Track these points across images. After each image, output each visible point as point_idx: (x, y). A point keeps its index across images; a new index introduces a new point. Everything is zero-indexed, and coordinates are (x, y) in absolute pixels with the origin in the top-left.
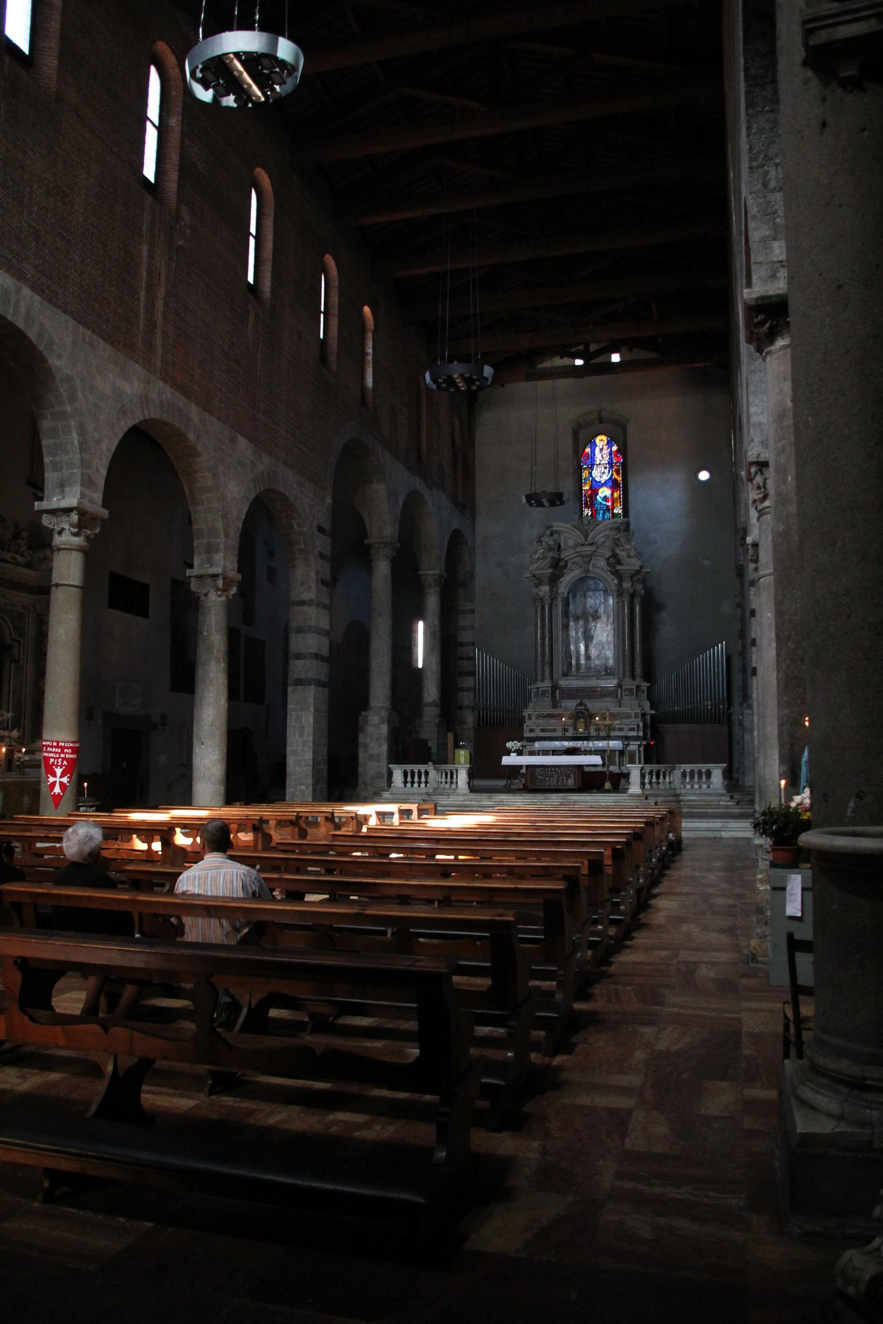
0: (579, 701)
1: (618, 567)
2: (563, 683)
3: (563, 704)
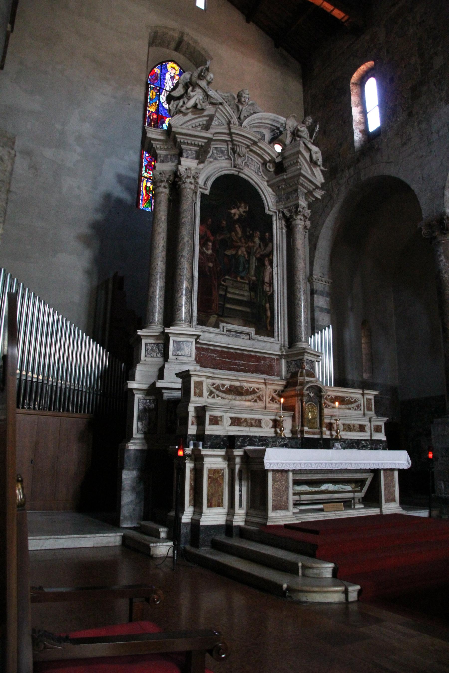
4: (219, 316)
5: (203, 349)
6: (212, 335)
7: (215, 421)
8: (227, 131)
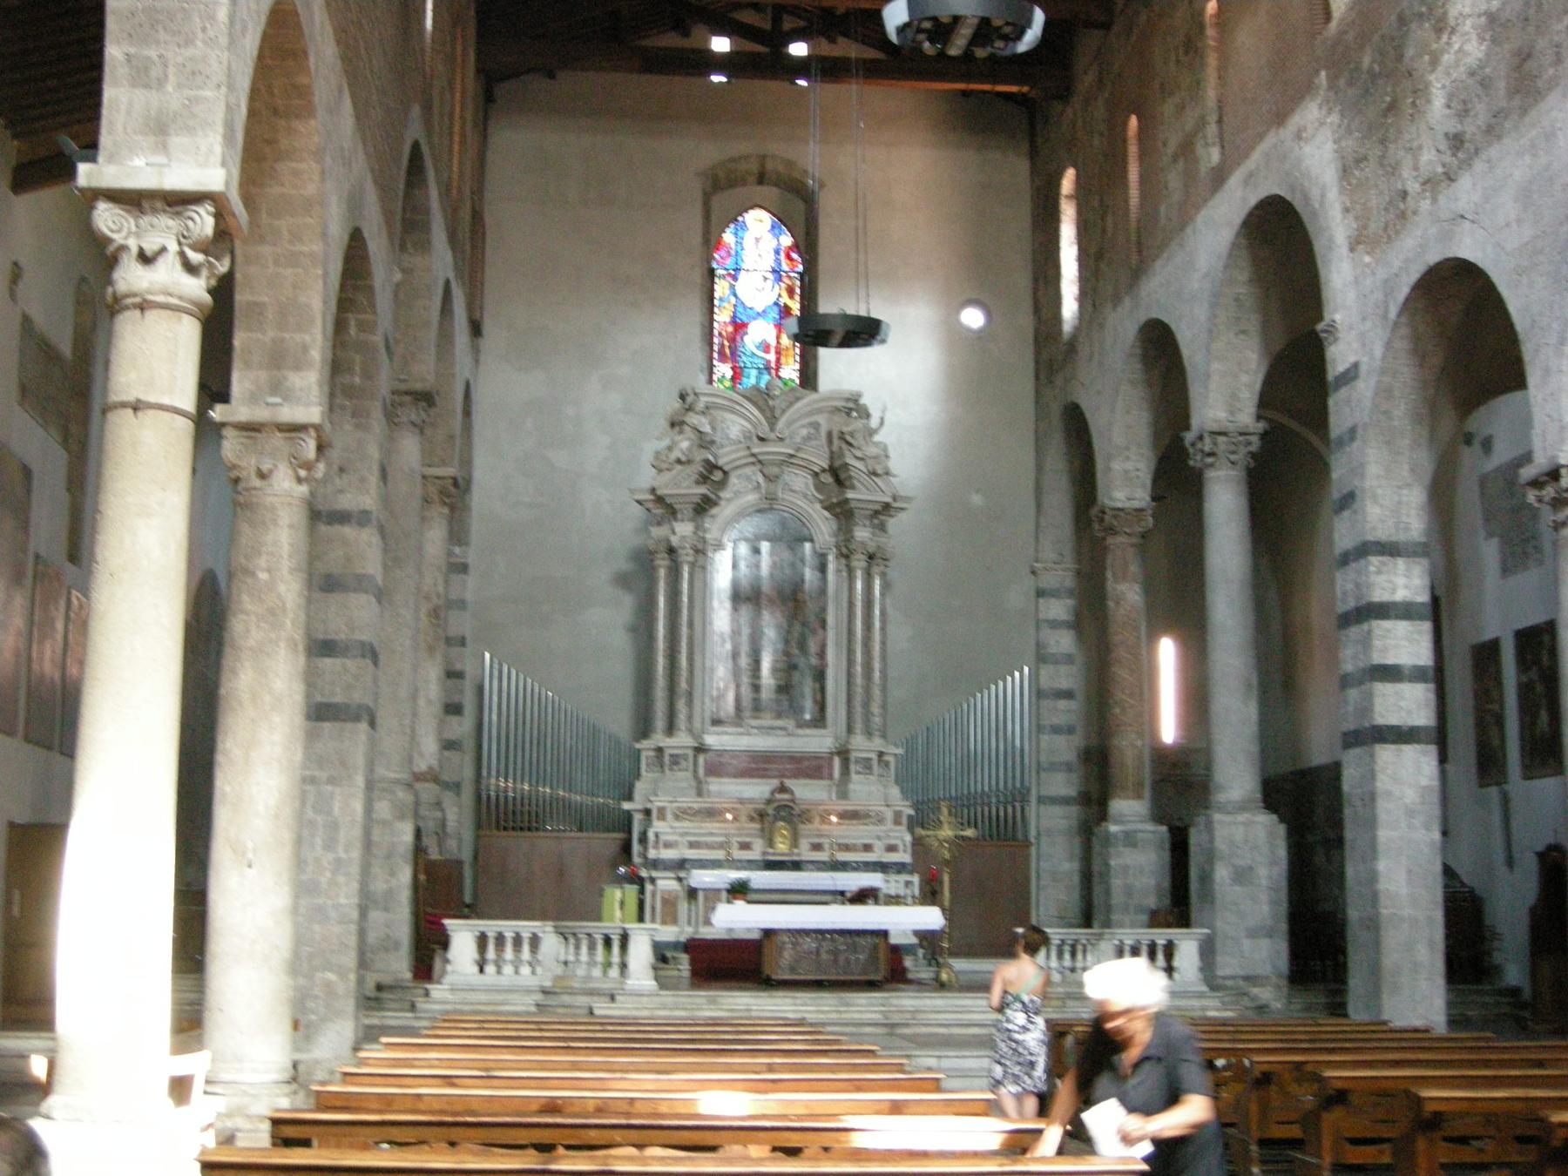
0: (775, 782)
1: (850, 495)
2: (711, 740)
3: (713, 788)
7: (668, 845)
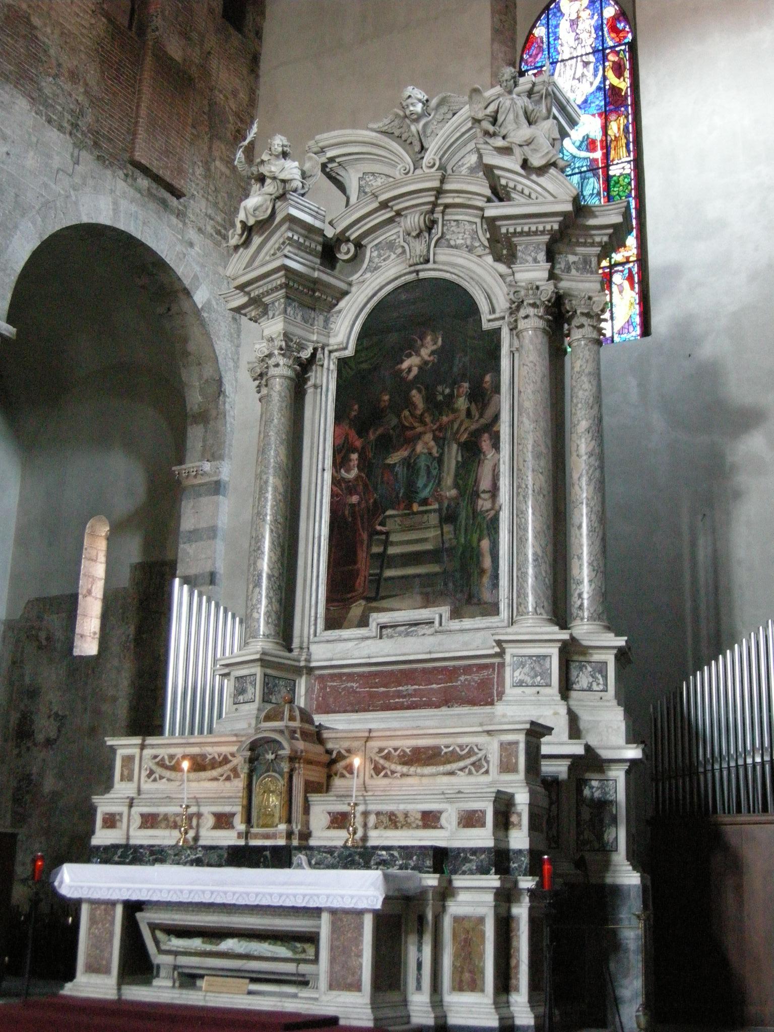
4: (369, 599)
5: (332, 677)
6: (350, 645)
8: (375, 205)
